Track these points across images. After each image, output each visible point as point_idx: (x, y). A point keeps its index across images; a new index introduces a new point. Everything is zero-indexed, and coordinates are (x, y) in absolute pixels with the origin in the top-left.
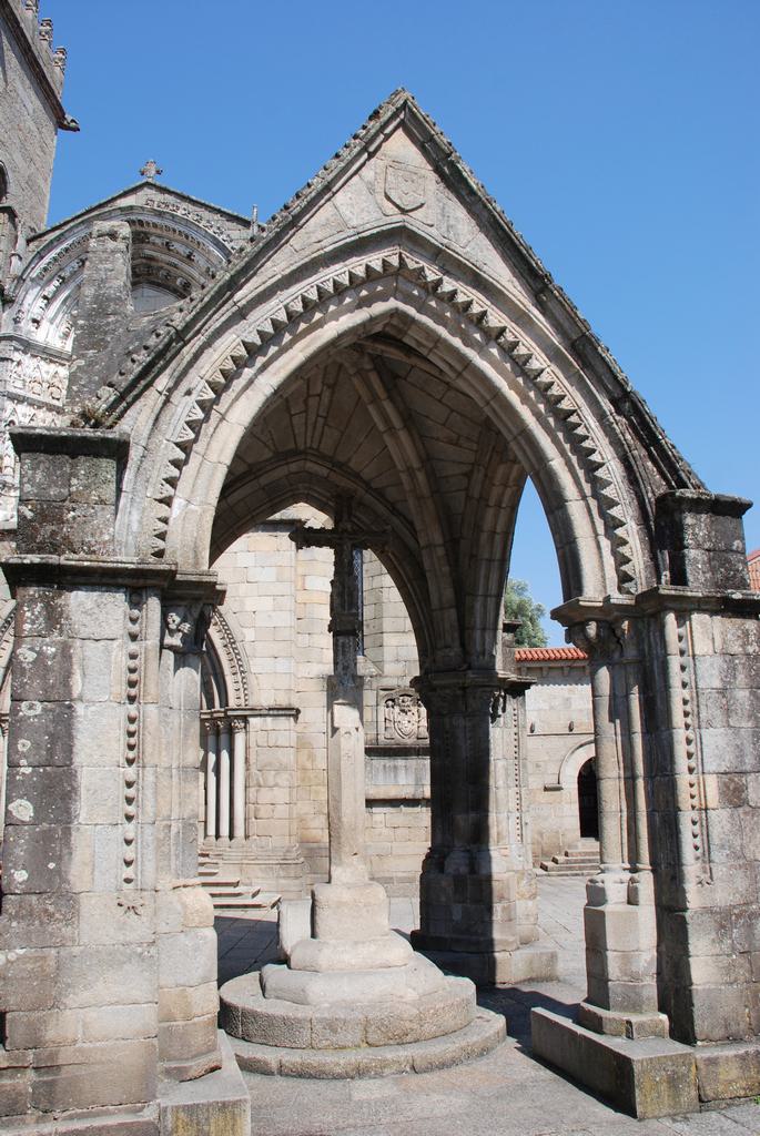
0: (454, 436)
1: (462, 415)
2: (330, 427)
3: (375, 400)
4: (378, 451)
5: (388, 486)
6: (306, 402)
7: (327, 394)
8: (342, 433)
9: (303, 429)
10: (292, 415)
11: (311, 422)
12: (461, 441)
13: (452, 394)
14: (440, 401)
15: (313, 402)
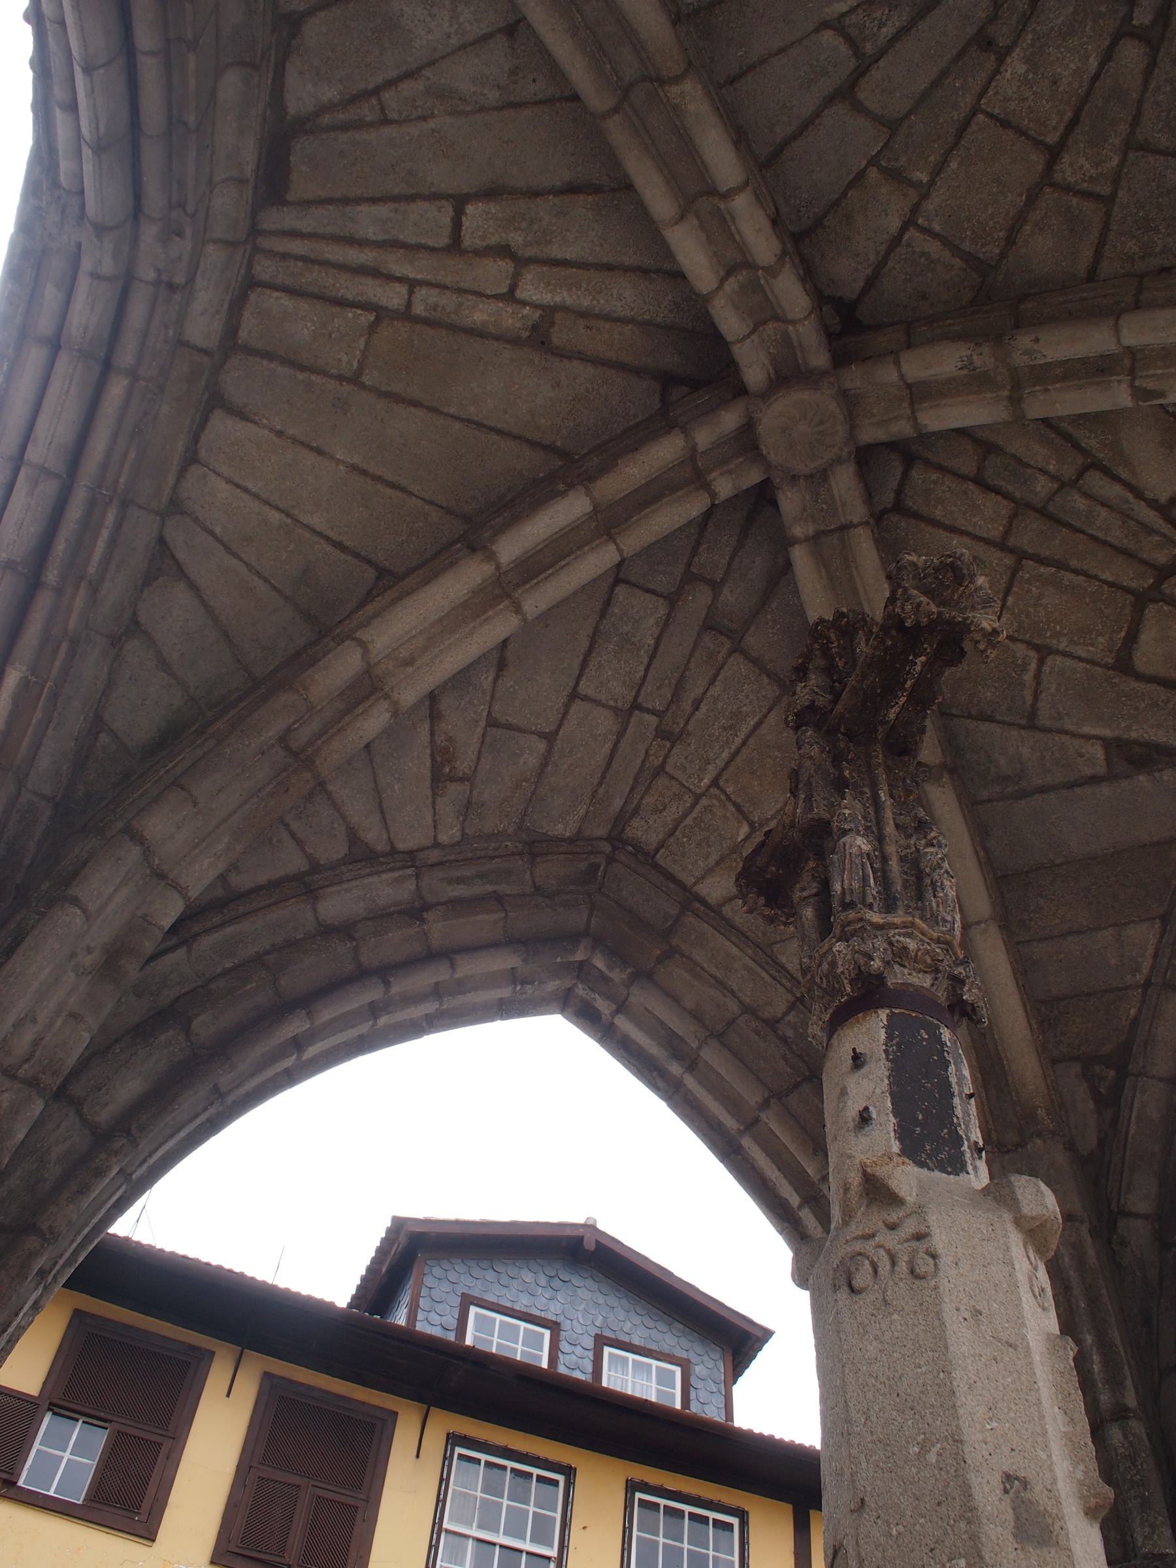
0: (464, 766)
1: (544, 765)
2: (373, 328)
3: (607, 522)
4: (317, 521)
5: (193, 586)
6: (504, 251)
7: (511, 319)
8: (355, 379)
9: (371, 232)
10: (460, 202)
11: (396, 264)
12: (454, 789)
13: (605, 723)
14: (574, 695)
15: (494, 273)
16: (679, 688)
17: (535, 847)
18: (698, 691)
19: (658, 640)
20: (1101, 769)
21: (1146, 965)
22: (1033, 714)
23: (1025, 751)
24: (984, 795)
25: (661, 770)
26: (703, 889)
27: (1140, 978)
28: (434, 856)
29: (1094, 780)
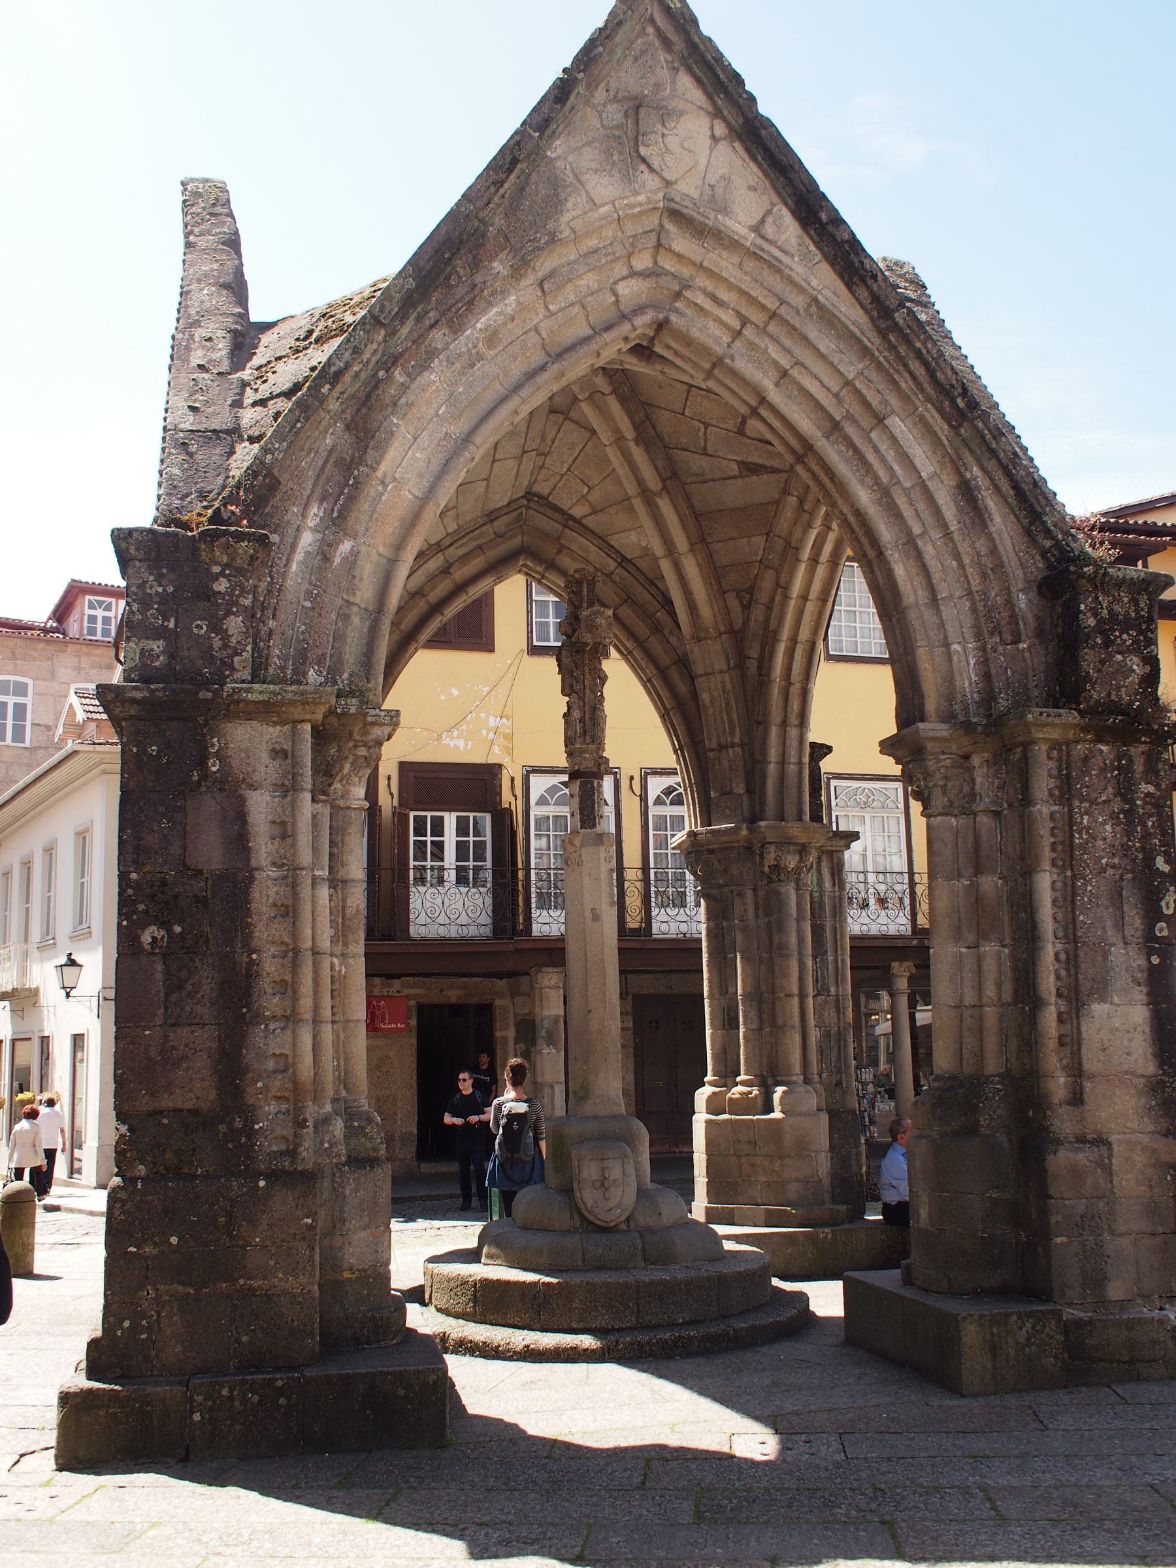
13: (512, 463)
14: (494, 461)
16: (543, 438)
17: (492, 516)
18: (552, 436)
19: (528, 428)
20: (736, 473)
21: (761, 553)
22: (705, 449)
23: (704, 464)
24: (689, 481)
25: (542, 466)
26: (572, 512)
27: (758, 558)
28: (448, 541)
29: (734, 477)
